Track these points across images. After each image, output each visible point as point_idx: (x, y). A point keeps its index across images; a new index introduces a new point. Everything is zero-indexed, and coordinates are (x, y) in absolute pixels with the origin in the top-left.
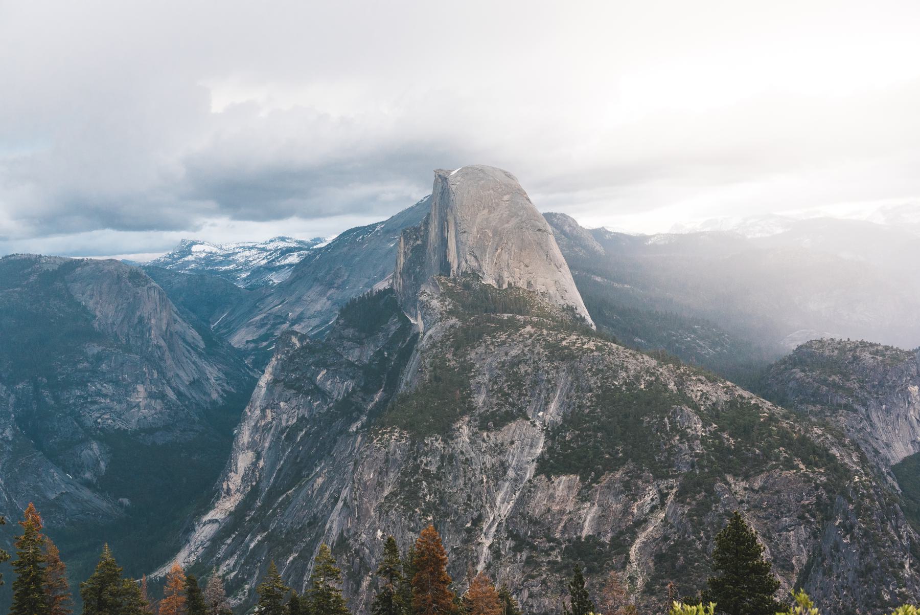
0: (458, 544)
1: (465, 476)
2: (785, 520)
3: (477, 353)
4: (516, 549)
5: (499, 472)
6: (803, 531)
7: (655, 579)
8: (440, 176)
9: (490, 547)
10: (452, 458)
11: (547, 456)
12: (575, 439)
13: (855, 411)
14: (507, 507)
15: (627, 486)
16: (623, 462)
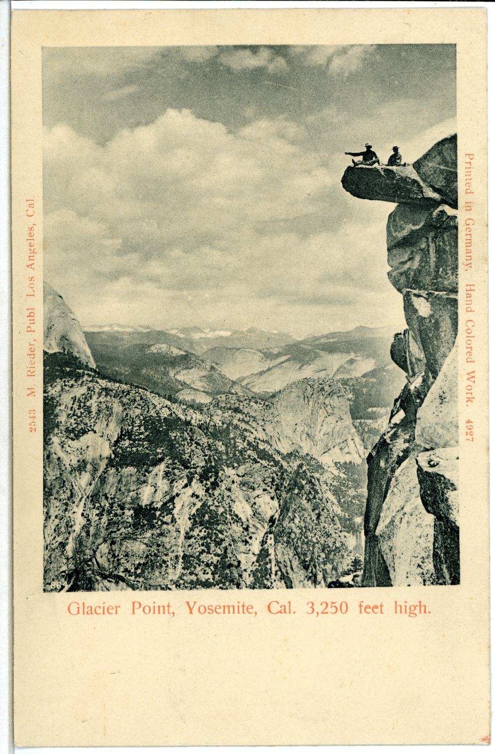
1: (60, 469)
2: (257, 492)
3: (56, 391)
7: (192, 529)
9: (83, 515)
11: (113, 456)
13: (252, 433)
14: (89, 488)
15: (167, 474)
16: (161, 460)
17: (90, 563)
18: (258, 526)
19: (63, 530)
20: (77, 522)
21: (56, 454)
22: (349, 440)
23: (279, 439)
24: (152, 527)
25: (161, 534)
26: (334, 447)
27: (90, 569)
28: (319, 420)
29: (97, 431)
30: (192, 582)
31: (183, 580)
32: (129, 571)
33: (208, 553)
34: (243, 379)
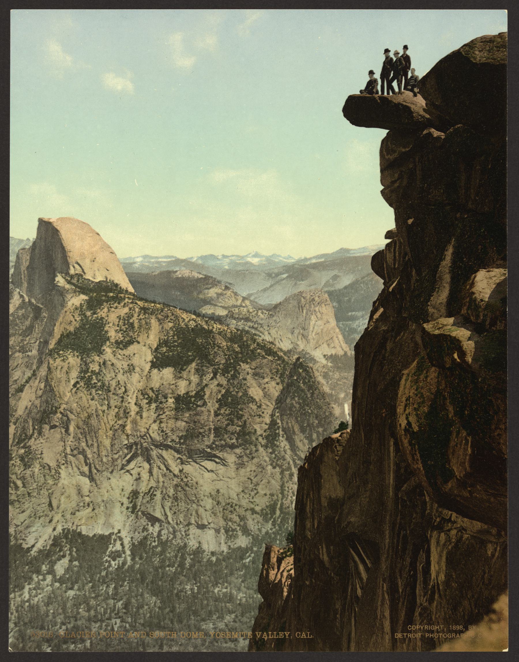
0: (119, 404)
2: (266, 380)
4: (149, 403)
5: (131, 369)
6: (273, 383)
7: (219, 409)
8: (45, 222)
9: (136, 404)
10: (104, 363)
11: (155, 360)
12: (167, 351)
13: (260, 336)
15: (197, 370)
16: (192, 361)
17: (145, 437)
18: (269, 404)
19: (122, 415)
20: (132, 409)
21: (110, 361)
22: (335, 338)
23: (281, 340)
24: (189, 409)
25: (197, 414)
26: (323, 344)
27: (146, 442)
28: (311, 323)
29: (141, 342)
30: (222, 446)
31: (215, 444)
32: (175, 441)
33: (233, 425)
34: (250, 295)
